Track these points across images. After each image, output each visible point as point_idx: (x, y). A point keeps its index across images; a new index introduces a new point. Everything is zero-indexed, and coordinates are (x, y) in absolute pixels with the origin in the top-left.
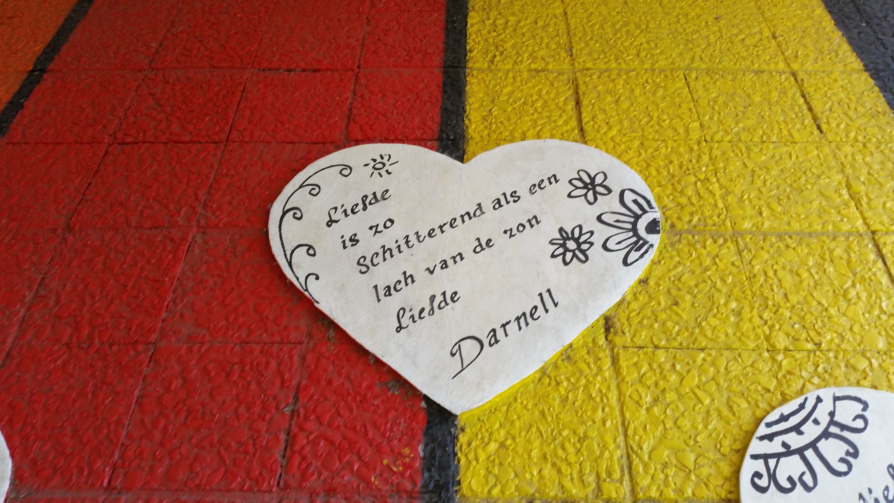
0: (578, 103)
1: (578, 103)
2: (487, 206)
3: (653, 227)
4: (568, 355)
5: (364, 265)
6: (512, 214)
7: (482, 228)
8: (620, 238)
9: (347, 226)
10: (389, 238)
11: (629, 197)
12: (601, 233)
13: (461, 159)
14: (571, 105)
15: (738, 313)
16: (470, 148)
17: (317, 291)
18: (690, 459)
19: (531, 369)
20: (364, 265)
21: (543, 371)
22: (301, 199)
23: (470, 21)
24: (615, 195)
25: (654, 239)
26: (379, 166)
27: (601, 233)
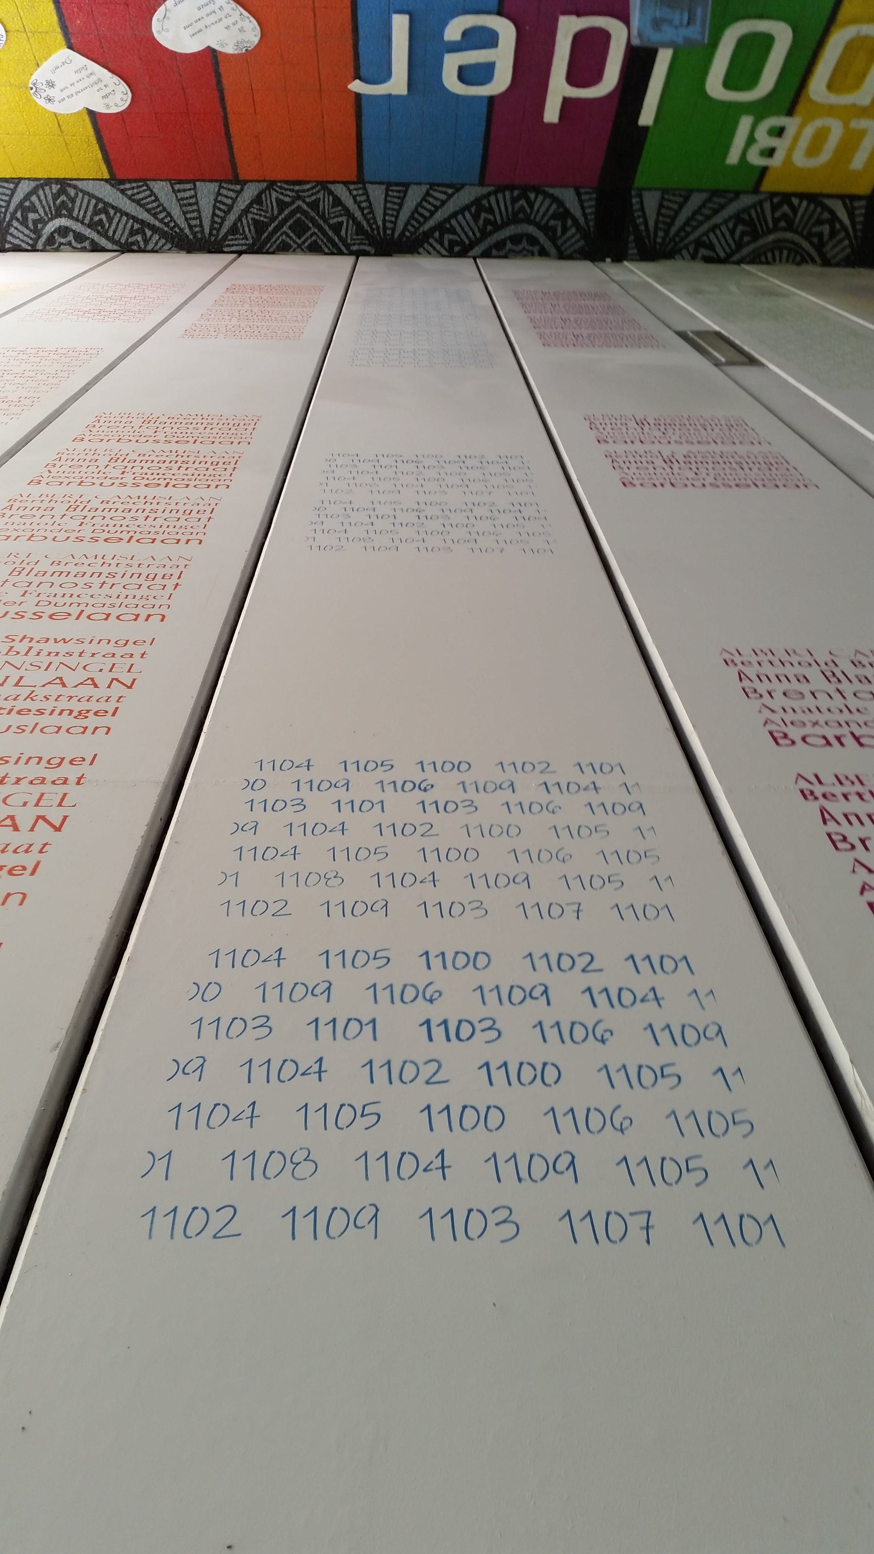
0: (59, 125)
1: (59, 125)
2: (74, 95)
3: (32, 89)
4: (46, 59)
5: (100, 80)
6: (67, 92)
7: (72, 90)
8: (39, 86)
9: (108, 90)
10: (96, 87)
11: (39, 97)
12: (44, 87)
13: (87, 109)
14: (61, 124)
15: (9, 67)
16: (85, 111)
17: (110, 74)
18: (16, 39)
19: (53, 56)
20: (100, 80)
21: (50, 56)
22: (125, 97)
23: (100, 154)
24: (43, 97)
25: (31, 86)
26: (108, 106)
27: (44, 87)
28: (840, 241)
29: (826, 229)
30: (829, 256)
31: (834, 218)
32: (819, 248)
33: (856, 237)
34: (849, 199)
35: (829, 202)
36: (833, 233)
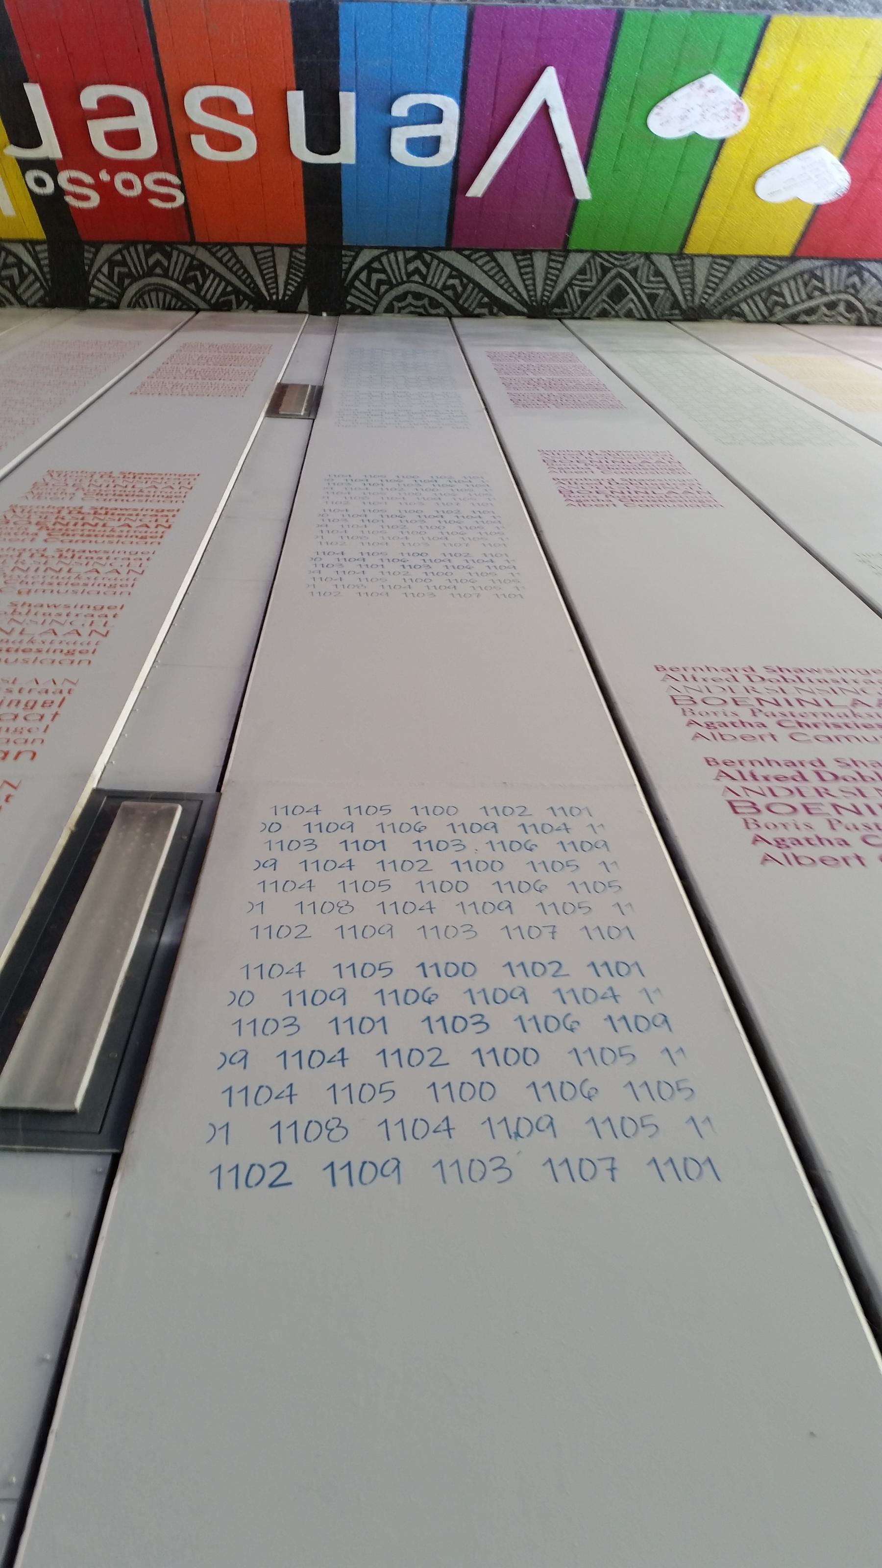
28: (31, 285)
29: (15, 272)
30: (24, 297)
31: (20, 262)
32: (13, 289)
33: (46, 280)
34: (30, 244)
35: (14, 248)
36: (23, 277)
